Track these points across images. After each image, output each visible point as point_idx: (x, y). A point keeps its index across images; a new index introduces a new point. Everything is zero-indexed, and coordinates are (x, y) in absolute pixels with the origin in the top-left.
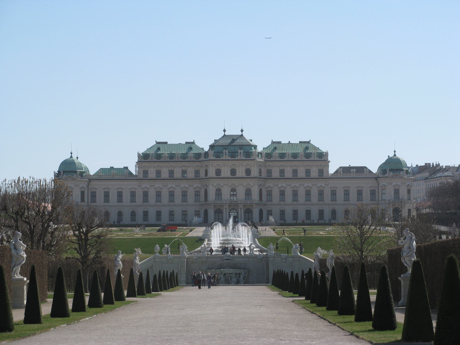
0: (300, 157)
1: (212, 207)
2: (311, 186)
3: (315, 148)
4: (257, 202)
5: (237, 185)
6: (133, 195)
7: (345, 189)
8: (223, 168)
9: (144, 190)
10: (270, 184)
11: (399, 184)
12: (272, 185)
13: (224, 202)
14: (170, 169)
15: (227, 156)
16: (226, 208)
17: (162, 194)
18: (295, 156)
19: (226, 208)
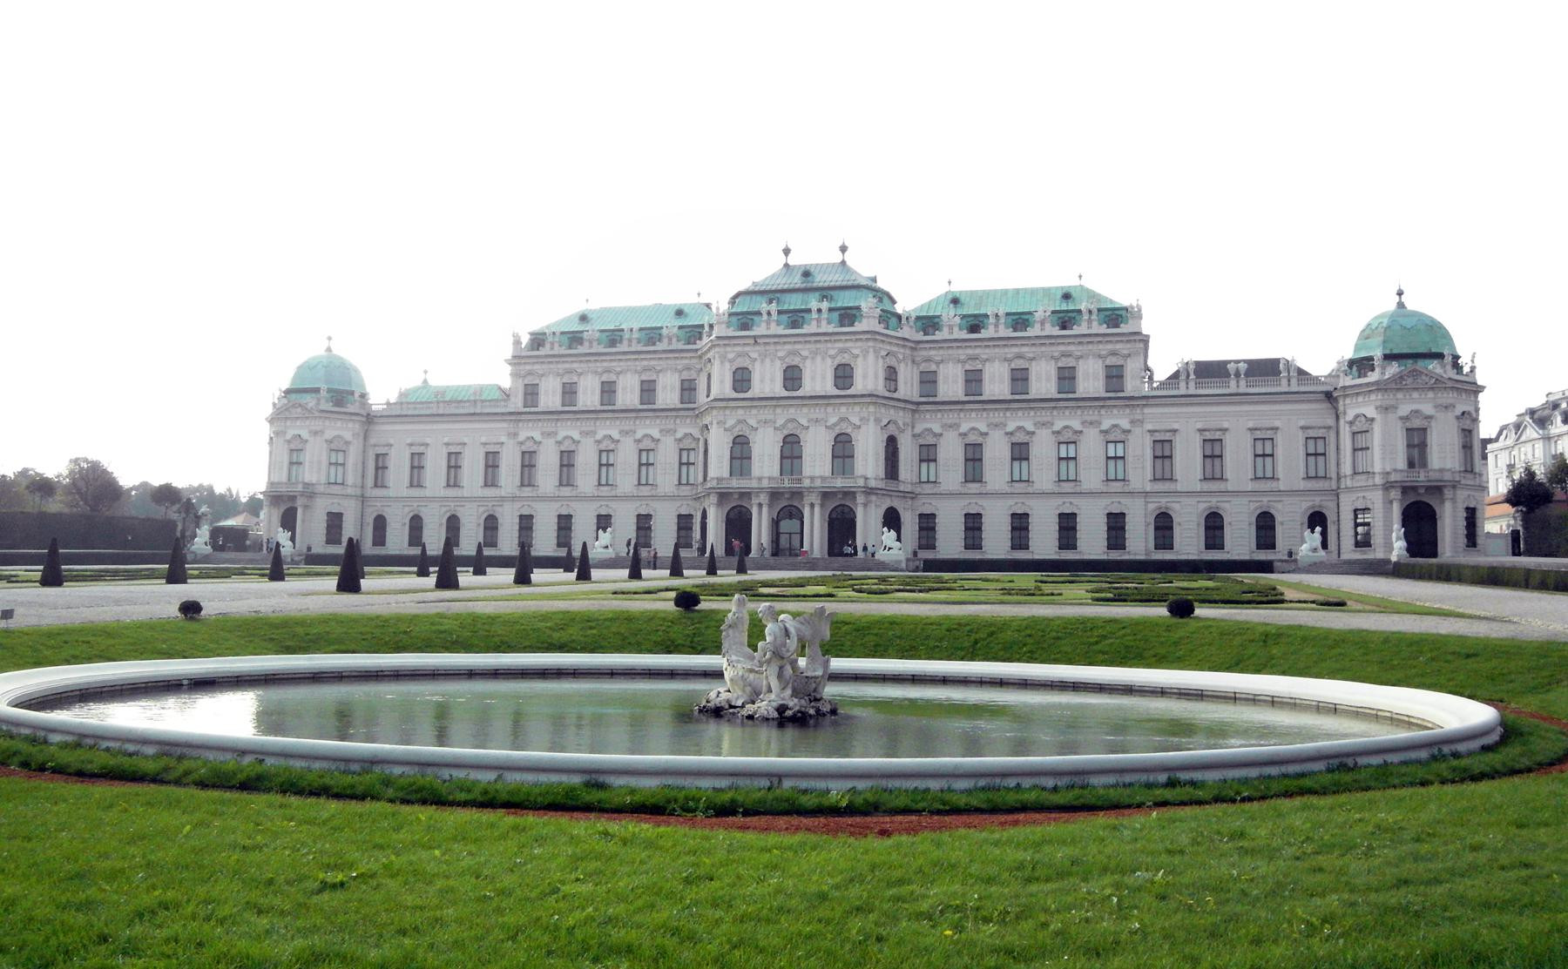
0: (1037, 326)
1: (714, 499)
2: (1076, 425)
3: (1093, 296)
4: (872, 484)
5: (804, 422)
6: (492, 463)
7: (1208, 436)
8: (757, 365)
9: (524, 448)
10: (931, 423)
11: (1427, 409)
12: (937, 429)
13: (754, 484)
14: (605, 378)
15: (773, 325)
16: (760, 505)
18: (1020, 321)
19: (760, 505)
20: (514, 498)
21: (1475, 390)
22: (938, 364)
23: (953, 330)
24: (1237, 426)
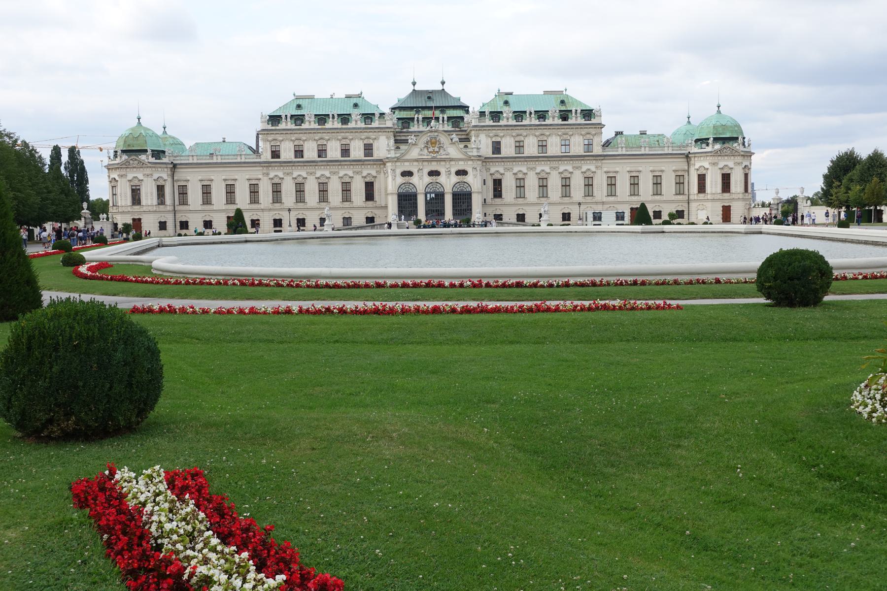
2: (571, 170)
9: (274, 181)
11: (731, 164)
12: (502, 171)
14: (319, 143)
17: (307, 188)
18: (542, 115)
20: (270, 210)
21: (749, 155)
22: (502, 137)
23: (508, 120)
24: (646, 170)
